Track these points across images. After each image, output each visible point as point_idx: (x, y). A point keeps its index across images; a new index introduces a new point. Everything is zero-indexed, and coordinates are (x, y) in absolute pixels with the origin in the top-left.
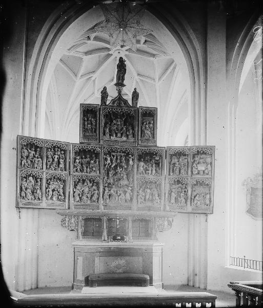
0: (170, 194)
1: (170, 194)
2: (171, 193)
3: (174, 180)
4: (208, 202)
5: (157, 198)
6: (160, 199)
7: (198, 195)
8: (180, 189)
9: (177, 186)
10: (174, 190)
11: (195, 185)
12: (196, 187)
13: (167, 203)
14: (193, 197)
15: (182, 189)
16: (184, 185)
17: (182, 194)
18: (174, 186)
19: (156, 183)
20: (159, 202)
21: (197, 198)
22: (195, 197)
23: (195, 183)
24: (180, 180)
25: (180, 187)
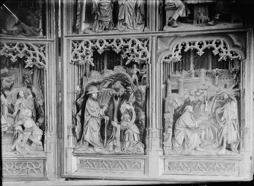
0: (81, 108)
1: (81, 108)
2: (84, 103)
3: (95, 50)
4: (232, 136)
5: (30, 123)
6: (43, 127)
7: (190, 108)
8: (118, 84)
9: (108, 73)
10: (94, 91)
11: (179, 66)
12: (182, 76)
13: (69, 142)
14: (169, 117)
15: (126, 84)
16: (135, 70)
17: (126, 106)
18: (95, 76)
19: (21, 62)
20: (37, 140)
21: (186, 118)
22: (177, 117)
23: (178, 58)
24: (118, 50)
25: (119, 77)
